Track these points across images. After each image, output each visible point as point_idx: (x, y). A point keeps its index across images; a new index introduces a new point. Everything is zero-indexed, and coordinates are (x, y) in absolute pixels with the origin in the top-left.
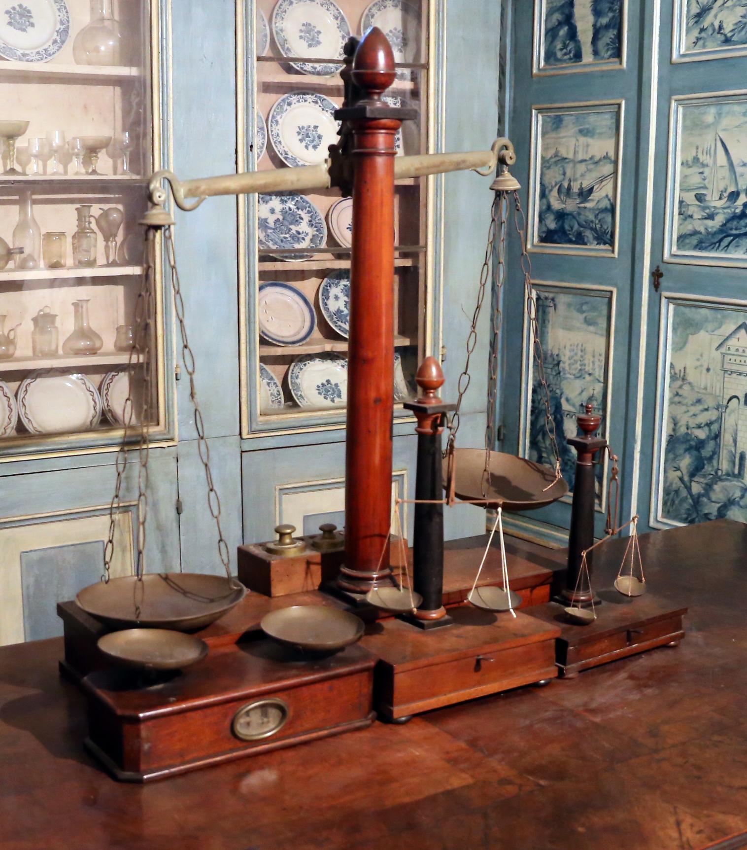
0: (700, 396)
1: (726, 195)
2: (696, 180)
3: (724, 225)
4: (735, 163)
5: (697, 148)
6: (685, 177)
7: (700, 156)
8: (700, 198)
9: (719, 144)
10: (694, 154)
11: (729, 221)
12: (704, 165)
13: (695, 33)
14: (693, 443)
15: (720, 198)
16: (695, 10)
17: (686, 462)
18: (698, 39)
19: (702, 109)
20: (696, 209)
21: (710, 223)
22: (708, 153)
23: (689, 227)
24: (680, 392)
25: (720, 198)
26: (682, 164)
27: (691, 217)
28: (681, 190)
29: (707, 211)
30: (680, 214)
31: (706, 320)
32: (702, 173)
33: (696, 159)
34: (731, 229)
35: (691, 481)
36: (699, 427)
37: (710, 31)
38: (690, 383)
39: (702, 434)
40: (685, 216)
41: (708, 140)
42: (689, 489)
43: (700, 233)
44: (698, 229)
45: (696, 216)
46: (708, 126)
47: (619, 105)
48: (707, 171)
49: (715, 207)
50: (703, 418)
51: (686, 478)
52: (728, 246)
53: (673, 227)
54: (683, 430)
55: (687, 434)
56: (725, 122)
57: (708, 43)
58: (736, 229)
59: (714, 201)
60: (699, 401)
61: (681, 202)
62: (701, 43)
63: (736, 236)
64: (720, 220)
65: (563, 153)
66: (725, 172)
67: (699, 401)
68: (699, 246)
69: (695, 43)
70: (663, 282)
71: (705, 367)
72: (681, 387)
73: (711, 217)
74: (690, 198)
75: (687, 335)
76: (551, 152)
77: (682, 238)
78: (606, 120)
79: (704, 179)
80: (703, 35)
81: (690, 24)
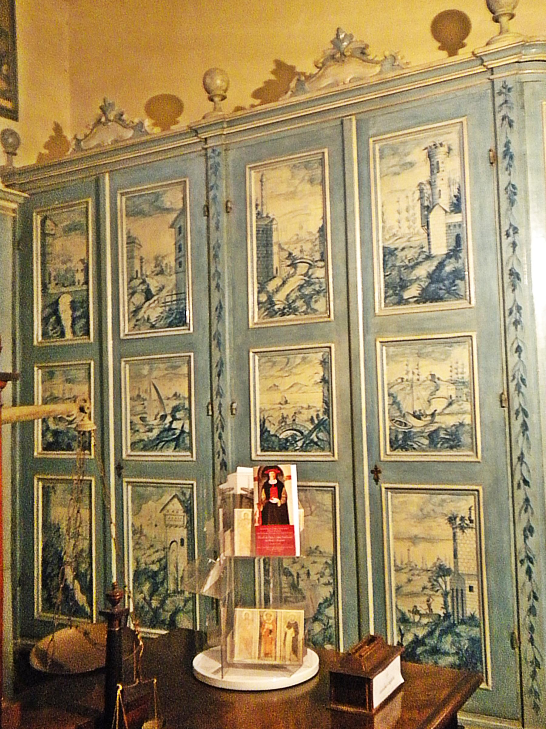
0: (152, 543)
1: (159, 417)
2: (139, 408)
3: (158, 435)
4: (163, 398)
5: (139, 389)
6: (133, 407)
7: (141, 394)
8: (143, 419)
9: (152, 387)
10: (137, 393)
11: (161, 432)
12: (144, 400)
13: (133, 322)
14: (150, 574)
15: (155, 419)
16: (133, 308)
17: (146, 587)
18: (136, 325)
19: (141, 366)
20: (141, 426)
21: (150, 434)
22: (146, 392)
23: (137, 437)
24: (140, 541)
25: (155, 419)
26: (131, 399)
27: (138, 431)
28: (131, 415)
29: (148, 427)
30: (131, 429)
31: (152, 494)
32: (143, 404)
33: (139, 396)
34: (163, 437)
35: (151, 599)
36: (153, 563)
37: (142, 320)
38: (145, 536)
39: (155, 568)
40: (135, 431)
41: (145, 385)
42: (150, 605)
43: (143, 440)
44: (143, 438)
45: (141, 430)
46: (145, 376)
47: (90, 364)
48: (146, 403)
49: (153, 425)
50: (155, 557)
51: (148, 598)
52: (162, 447)
53: (127, 438)
54: (143, 566)
55: (145, 569)
56: (155, 374)
57: (142, 328)
58: (167, 437)
59: (152, 421)
60: (152, 546)
61: (131, 422)
62: (137, 327)
63: (167, 441)
64: (156, 432)
65: (56, 393)
66: (157, 403)
67: (152, 546)
68: (144, 449)
69: (134, 328)
70: (124, 472)
71: (154, 524)
72: (139, 538)
73: (150, 430)
74: (137, 419)
75: (141, 505)
76: (48, 394)
77: (133, 444)
78: (81, 374)
79: (145, 408)
80: (138, 323)
81: (130, 316)
